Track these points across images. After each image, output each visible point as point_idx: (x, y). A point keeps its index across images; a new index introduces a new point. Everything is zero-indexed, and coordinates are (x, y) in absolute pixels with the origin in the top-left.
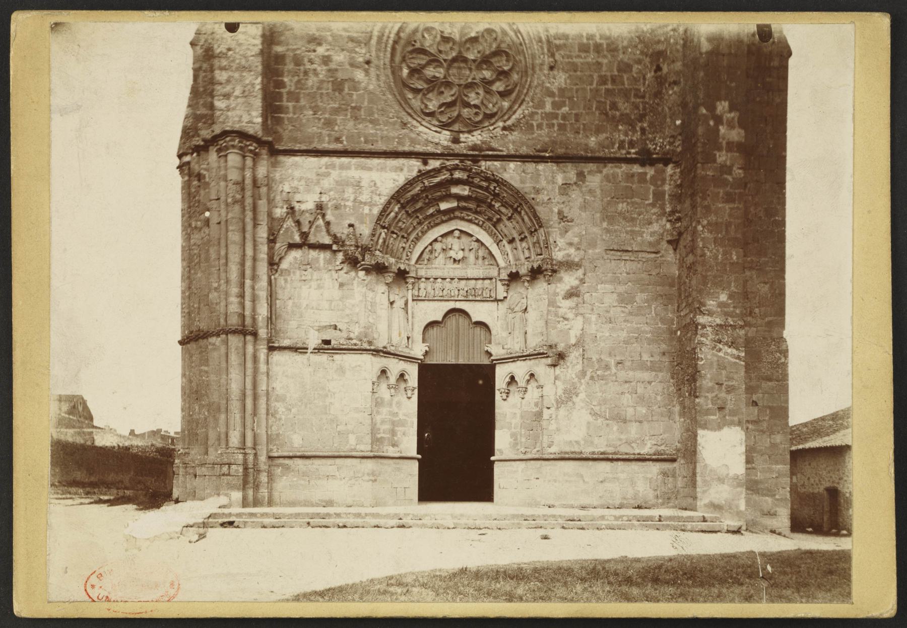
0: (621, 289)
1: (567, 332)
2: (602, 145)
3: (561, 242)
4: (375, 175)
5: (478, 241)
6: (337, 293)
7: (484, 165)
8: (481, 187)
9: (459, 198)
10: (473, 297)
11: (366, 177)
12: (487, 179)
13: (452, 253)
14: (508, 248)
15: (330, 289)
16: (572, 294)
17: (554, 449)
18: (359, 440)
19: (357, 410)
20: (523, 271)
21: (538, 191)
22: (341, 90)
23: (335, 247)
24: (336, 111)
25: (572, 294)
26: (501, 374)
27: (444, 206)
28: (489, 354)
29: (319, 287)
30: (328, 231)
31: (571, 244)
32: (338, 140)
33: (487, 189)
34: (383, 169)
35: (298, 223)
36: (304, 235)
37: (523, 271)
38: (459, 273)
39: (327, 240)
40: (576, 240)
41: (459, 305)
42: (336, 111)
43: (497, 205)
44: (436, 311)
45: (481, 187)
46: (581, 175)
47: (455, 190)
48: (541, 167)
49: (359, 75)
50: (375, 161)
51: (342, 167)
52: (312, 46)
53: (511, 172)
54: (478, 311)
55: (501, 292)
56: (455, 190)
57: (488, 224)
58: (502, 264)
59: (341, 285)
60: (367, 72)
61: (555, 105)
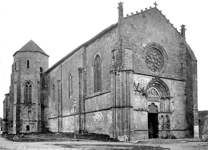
0: (179, 102)
1: (172, 109)
2: (175, 77)
3: (171, 93)
4: (146, 79)
5: (156, 91)
6: (140, 100)
7: (161, 79)
8: (160, 82)
9: (156, 84)
10: (156, 101)
11: (145, 79)
12: (162, 81)
13: (153, 93)
14: (161, 93)
15: (140, 99)
16: (173, 102)
17: (171, 129)
18: (145, 127)
19: (145, 122)
20: (165, 97)
21: (168, 84)
22: (139, 62)
23: (141, 92)
24: (139, 66)
25: (173, 102)
26: (160, 115)
27: (153, 85)
28: (157, 111)
29: (138, 99)
30: (141, 89)
31: (172, 94)
32: (139, 71)
33: (161, 83)
34: (147, 78)
35: (136, 86)
36: (137, 89)
37: (165, 97)
38: (154, 97)
39: (140, 90)
40: (173, 93)
41: (153, 102)
42: (139, 66)
43: (161, 86)
44: (150, 103)
45: (160, 82)
46: (173, 82)
47: (156, 82)
48: (168, 80)
49: (142, 60)
50: (147, 76)
51: (142, 77)
52: (135, 53)
53: (164, 80)
54: (157, 104)
55: (160, 101)
56: (156, 82)
57: (158, 88)
58: (159, 95)
59: (141, 98)
60: (143, 59)
61: (169, 69)
